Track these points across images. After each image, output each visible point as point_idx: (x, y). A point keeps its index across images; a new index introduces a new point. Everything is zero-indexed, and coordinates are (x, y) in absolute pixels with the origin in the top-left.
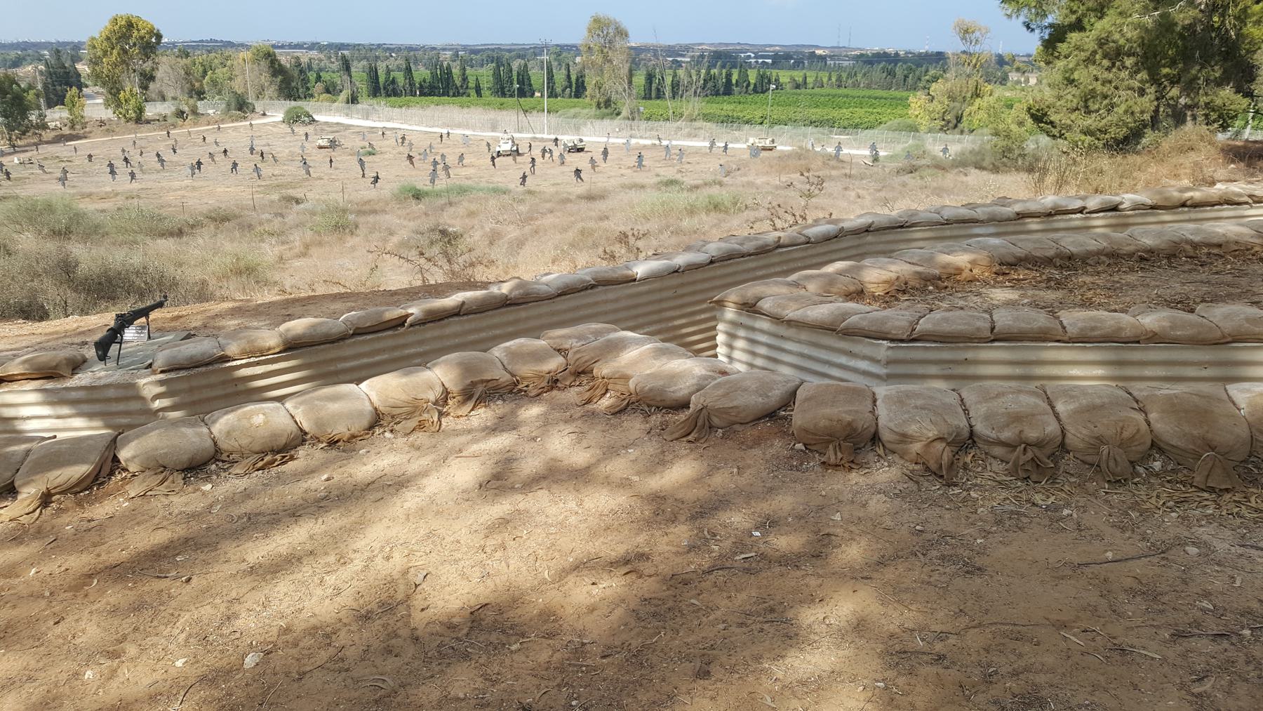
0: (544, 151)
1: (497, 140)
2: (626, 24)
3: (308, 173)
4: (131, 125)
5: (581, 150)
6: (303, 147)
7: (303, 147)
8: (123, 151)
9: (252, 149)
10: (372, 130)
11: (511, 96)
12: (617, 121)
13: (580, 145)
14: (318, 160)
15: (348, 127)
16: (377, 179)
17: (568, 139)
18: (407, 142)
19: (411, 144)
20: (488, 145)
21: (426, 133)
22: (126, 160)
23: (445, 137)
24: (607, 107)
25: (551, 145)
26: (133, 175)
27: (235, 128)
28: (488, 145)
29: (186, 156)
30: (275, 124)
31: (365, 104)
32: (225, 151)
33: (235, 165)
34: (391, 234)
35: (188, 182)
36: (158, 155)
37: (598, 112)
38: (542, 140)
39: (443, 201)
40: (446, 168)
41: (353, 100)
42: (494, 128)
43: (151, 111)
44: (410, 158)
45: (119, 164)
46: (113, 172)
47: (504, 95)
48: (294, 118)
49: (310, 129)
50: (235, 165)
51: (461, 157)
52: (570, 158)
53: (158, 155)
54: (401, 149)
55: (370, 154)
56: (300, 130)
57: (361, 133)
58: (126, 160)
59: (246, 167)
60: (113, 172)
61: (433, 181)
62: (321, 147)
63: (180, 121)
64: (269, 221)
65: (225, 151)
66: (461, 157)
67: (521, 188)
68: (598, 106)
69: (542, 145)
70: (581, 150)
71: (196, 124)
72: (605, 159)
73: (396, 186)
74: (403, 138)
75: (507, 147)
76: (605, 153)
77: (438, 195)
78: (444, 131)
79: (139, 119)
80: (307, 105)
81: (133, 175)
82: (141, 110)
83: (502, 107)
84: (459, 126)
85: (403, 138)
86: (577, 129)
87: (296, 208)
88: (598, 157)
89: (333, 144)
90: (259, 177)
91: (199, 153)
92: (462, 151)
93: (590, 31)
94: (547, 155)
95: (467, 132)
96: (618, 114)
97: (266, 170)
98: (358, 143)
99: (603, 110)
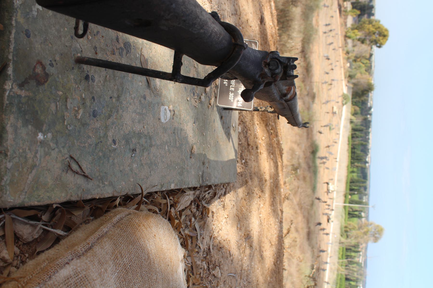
0: (329, 205)
1: (333, 184)
2: (380, 242)
3: (324, 103)
4: (344, 34)
5: (328, 221)
6: (333, 101)
7: (333, 101)
8: (334, 30)
9: (333, 80)
10: (339, 129)
11: (350, 186)
12: (339, 235)
13: (330, 221)
14: (329, 106)
15: (340, 119)
16: (320, 133)
17: (333, 214)
18: (334, 144)
19: (333, 146)
20: (332, 179)
21: (337, 152)
22: (331, 31)
23: (335, 160)
24: (345, 232)
25: (331, 208)
26: (325, 33)
27: (341, 74)
28: (332, 179)
29: (331, 54)
30: (342, 89)
31: (349, 126)
32: (332, 69)
33: (327, 73)
34: (298, 145)
35: (322, 54)
36: (332, 43)
37: (343, 227)
38: (333, 202)
39: (311, 164)
40: (324, 163)
41: (351, 122)
42: (339, 181)
43: (349, 41)
44: (328, 147)
45: (329, 28)
46: (327, 25)
47: (351, 182)
48: (345, 97)
49: (340, 104)
50: (327, 73)
51: (328, 168)
52: (325, 218)
53: (332, 43)
54: (331, 141)
55: (330, 129)
56: (340, 100)
57: (338, 125)
58: (331, 31)
59: (327, 78)
60: (327, 25)
61: (319, 158)
62: (333, 108)
63: (345, 52)
64: (306, 89)
65: (332, 69)
66: (328, 168)
67: (314, 198)
68: (346, 227)
69: (331, 204)
70: (328, 221)
71: (344, 58)
72: (324, 234)
73: (318, 142)
74: (336, 142)
75: (331, 187)
76: (327, 234)
77: (314, 162)
78: (338, 160)
79: (346, 37)
80: (350, 104)
81: (325, 33)
82: (349, 37)
83: (347, 183)
84: (340, 166)
85: (336, 142)
86: (336, 217)
87: (311, 101)
88: (325, 232)
89: (334, 113)
90: (323, 83)
91: (332, 58)
92: (330, 168)
93: (378, 226)
94: (327, 207)
95: (337, 170)
96: (342, 236)
97: (325, 86)
98: (334, 123)
99: (344, 229)
